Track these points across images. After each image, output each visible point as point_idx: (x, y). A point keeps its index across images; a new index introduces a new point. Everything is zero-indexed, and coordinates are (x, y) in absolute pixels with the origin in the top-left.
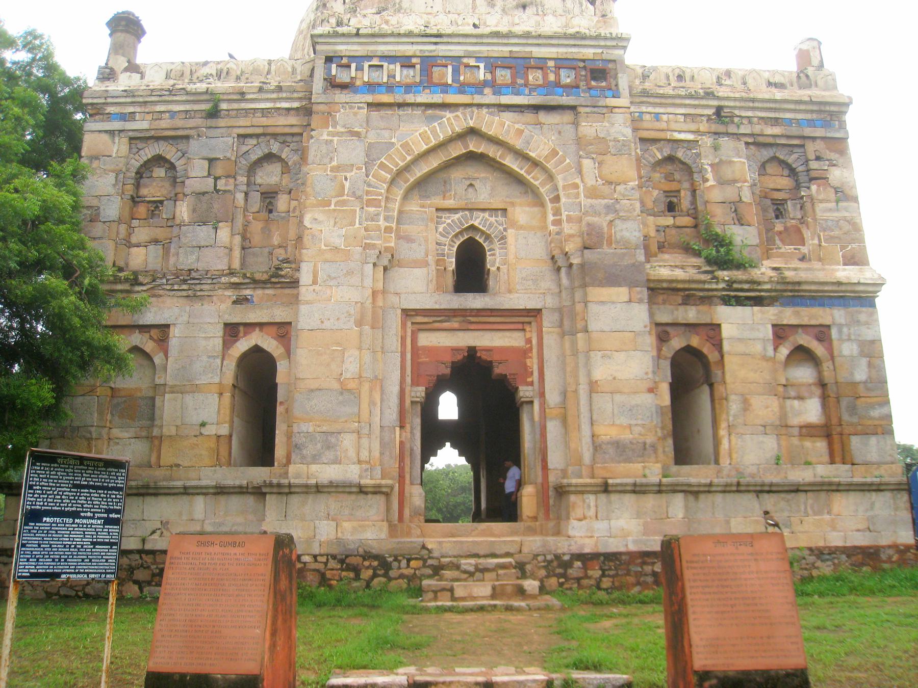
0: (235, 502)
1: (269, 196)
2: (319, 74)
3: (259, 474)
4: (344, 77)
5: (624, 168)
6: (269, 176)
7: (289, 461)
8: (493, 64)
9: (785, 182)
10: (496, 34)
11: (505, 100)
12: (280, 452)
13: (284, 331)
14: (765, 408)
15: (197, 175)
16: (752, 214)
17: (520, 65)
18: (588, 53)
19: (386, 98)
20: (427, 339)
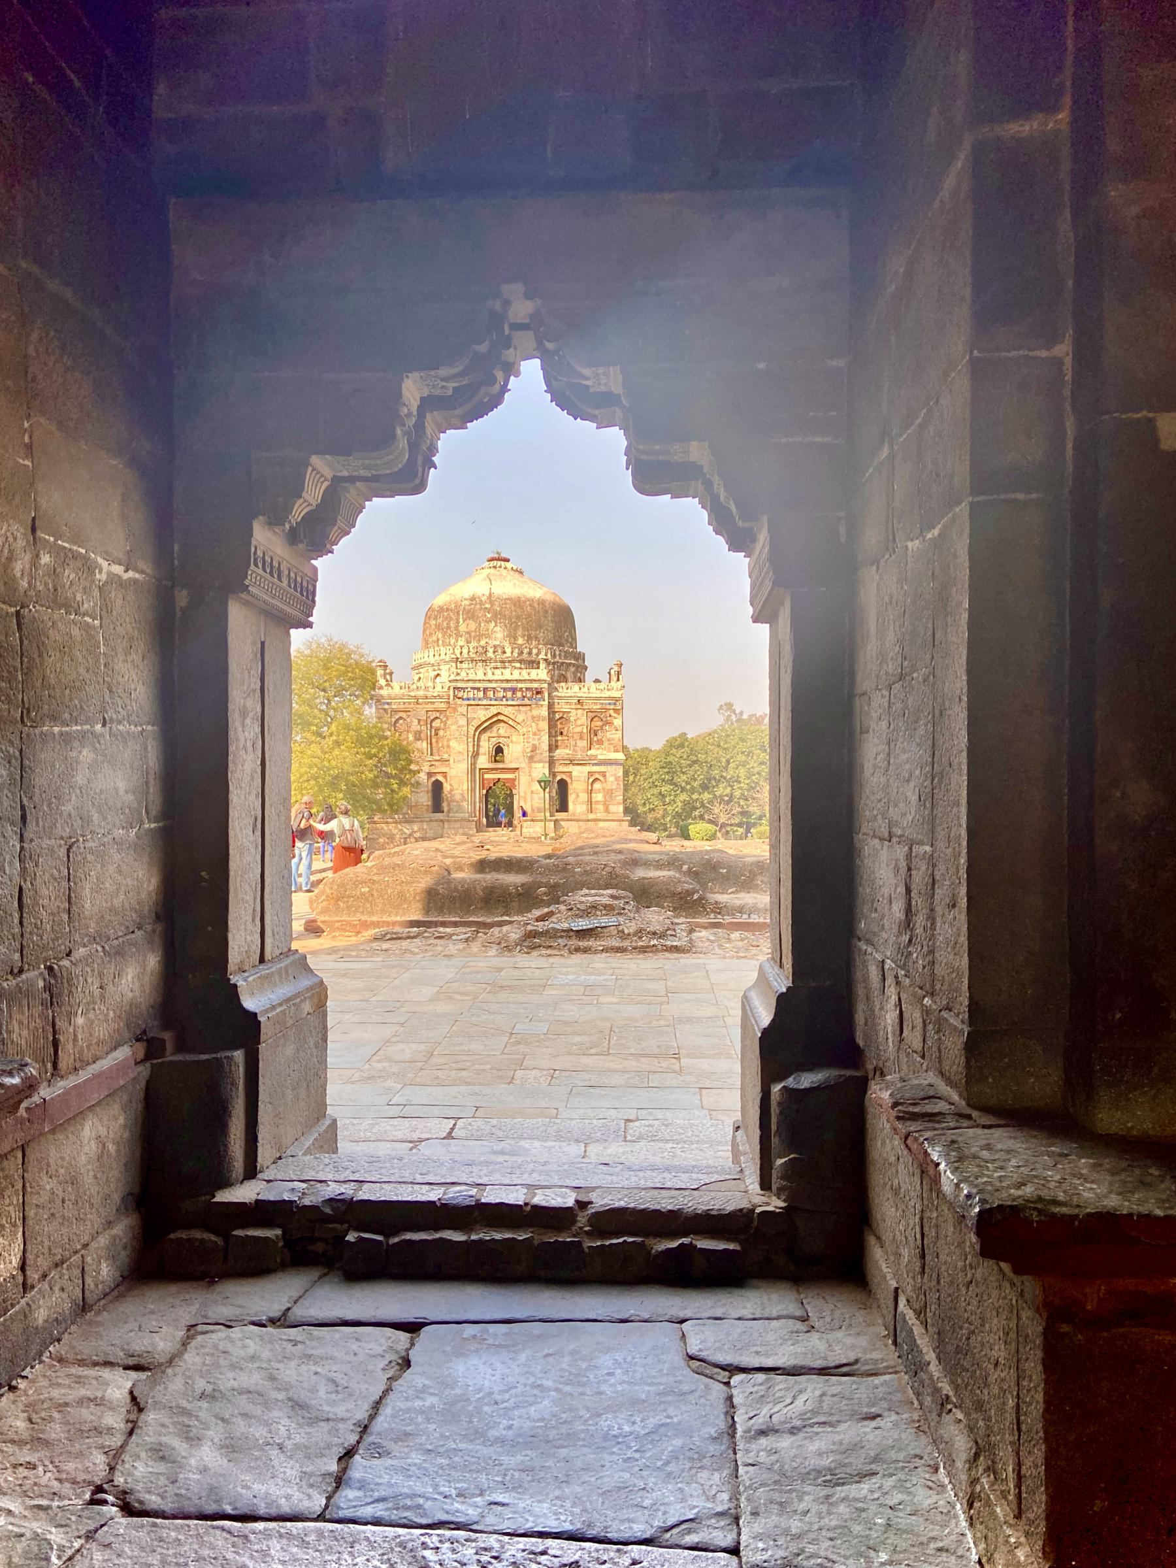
0: (435, 824)
1: (437, 730)
2: (451, 693)
3: (438, 816)
4: (460, 694)
5: (545, 725)
6: (436, 724)
7: (449, 812)
8: (505, 690)
9: (600, 723)
10: (507, 681)
11: (510, 703)
12: (446, 809)
13: (444, 774)
14: (584, 797)
15: (415, 725)
16: (585, 736)
17: (514, 690)
18: (535, 685)
19: (472, 702)
20: (486, 776)
